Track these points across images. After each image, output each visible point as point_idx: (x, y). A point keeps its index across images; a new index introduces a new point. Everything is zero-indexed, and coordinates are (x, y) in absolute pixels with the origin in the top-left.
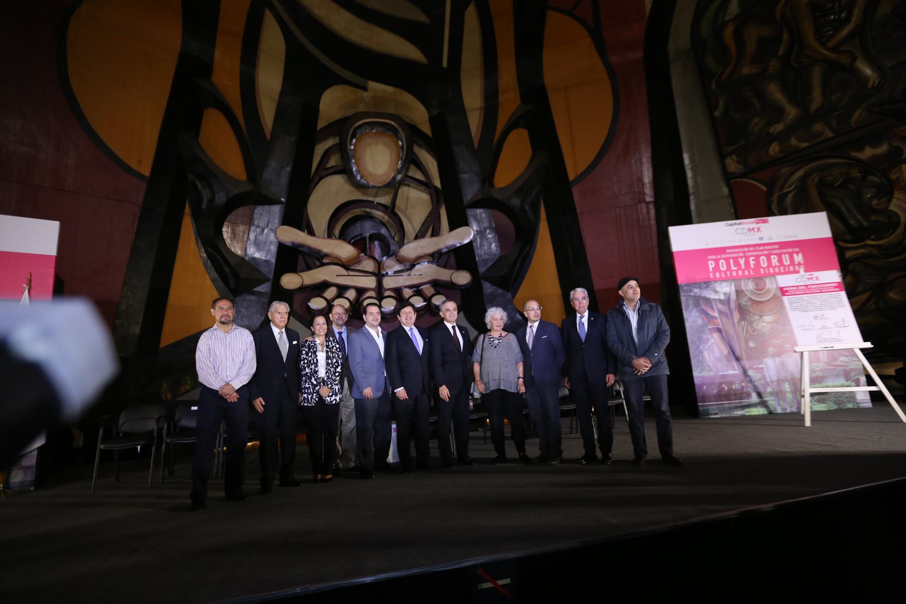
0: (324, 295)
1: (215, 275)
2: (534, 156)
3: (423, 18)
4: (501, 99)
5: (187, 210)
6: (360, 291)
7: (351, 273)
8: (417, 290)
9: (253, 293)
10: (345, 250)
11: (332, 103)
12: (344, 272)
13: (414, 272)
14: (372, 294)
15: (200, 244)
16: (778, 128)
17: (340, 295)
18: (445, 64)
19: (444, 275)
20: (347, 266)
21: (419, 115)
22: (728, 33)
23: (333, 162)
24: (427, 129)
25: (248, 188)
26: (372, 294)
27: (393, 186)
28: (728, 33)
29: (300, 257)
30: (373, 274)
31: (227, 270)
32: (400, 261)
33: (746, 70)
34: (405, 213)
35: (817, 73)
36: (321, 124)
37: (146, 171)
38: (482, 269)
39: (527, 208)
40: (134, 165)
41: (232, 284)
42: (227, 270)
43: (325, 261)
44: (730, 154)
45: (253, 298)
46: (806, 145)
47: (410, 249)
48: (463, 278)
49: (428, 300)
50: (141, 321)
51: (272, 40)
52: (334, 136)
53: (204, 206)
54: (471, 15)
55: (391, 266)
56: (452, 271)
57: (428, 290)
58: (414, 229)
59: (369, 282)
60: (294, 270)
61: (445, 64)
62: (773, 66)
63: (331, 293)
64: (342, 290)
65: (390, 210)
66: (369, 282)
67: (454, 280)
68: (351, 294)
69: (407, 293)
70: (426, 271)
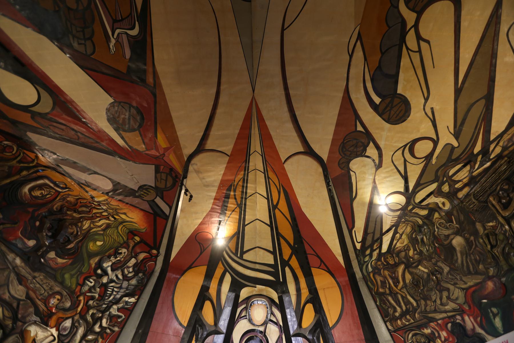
2: (315, 316)
3: (272, 270)
4: (302, 291)
5: (194, 338)
11: (244, 293)
16: (397, 314)
18: (281, 280)
21: (275, 296)
22: (371, 275)
23: (243, 315)
24: (277, 301)
25: (213, 329)
27: (265, 324)
28: (371, 275)
33: (381, 290)
34: (269, 335)
35: (399, 296)
36: (240, 300)
37: (185, 325)
39: (315, 338)
40: (183, 323)
44: (387, 321)
46: (407, 323)
51: (228, 279)
52: (244, 304)
54: (287, 269)
61: (281, 280)
62: (388, 291)
65: (264, 333)
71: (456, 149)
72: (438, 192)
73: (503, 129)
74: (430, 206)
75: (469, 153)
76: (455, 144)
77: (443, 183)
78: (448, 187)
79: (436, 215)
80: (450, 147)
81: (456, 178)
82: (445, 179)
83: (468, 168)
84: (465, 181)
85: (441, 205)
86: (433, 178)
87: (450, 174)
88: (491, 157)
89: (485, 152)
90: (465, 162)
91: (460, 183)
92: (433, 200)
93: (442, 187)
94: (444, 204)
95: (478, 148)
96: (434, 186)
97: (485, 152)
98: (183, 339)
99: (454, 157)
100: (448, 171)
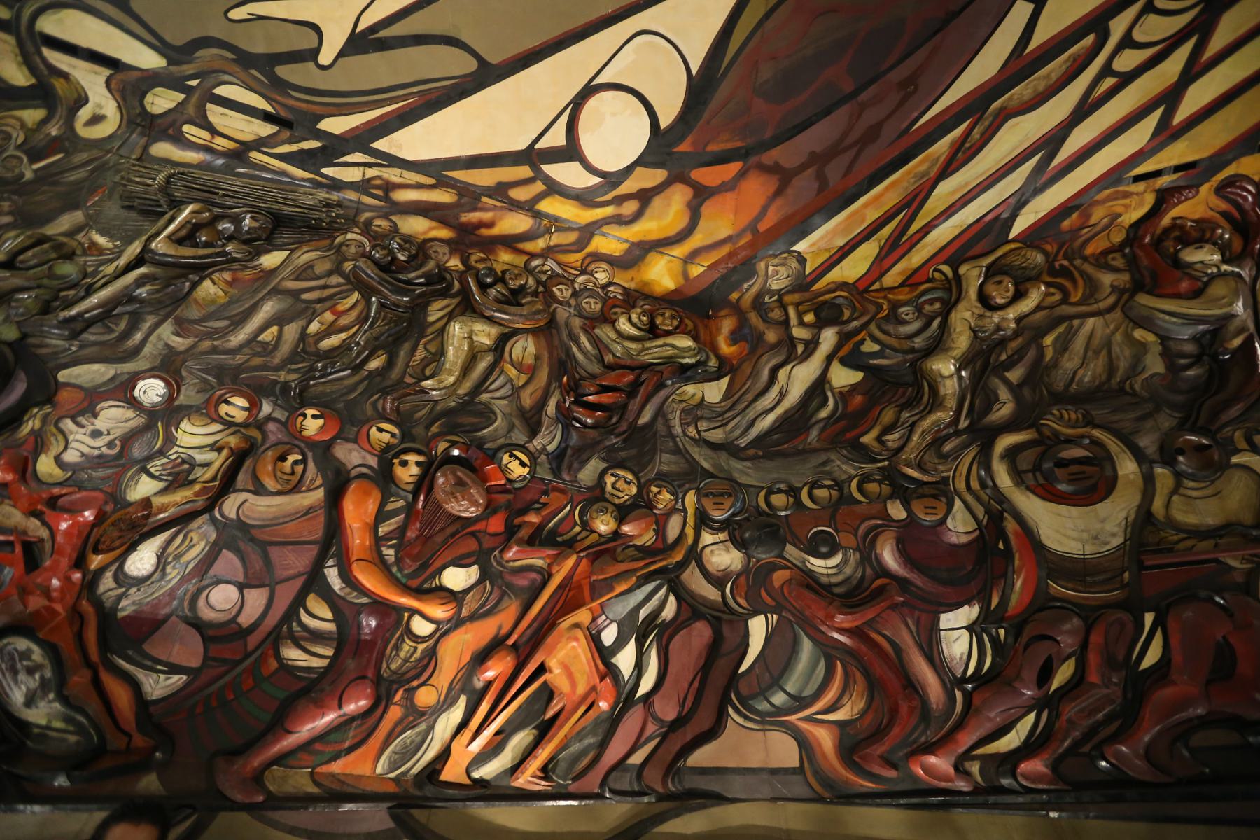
71: (311, 65)
72: (129, 85)
73: (411, 157)
74: (59, 84)
75: (314, 107)
76: (325, 57)
77: (176, 84)
78: (172, 105)
79: (32, 115)
80: (309, 41)
81: (216, 114)
82: (194, 83)
83: (267, 129)
84: (221, 143)
85: (84, 114)
86: (177, 37)
87: (221, 91)
88: (324, 171)
89: (334, 148)
90: (283, 113)
91: (205, 135)
92: (92, 80)
93: (158, 90)
94: (96, 119)
95: (335, 125)
96: (147, 59)
97: (334, 148)
99: (283, 71)
100: (226, 78)
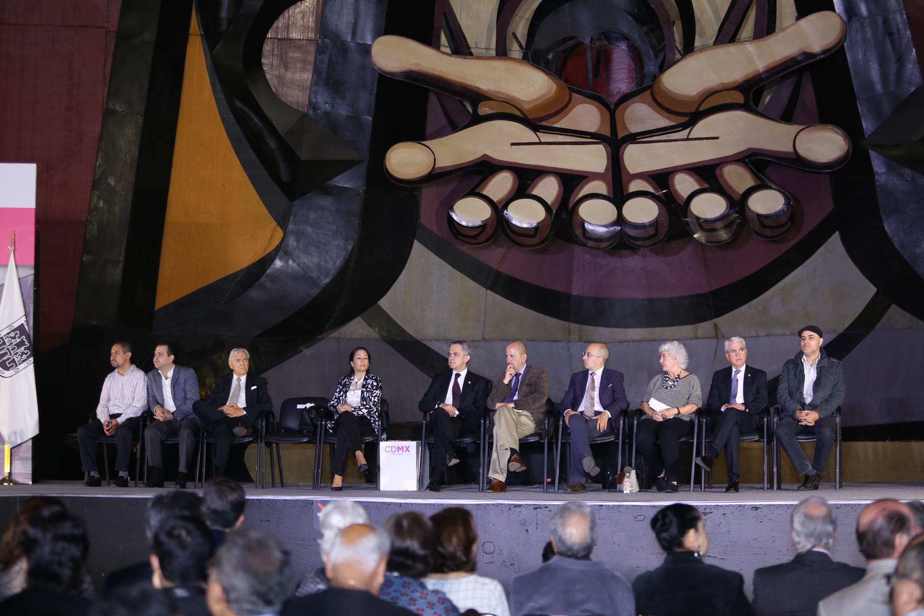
0: (485, 193)
1: (252, 155)
6: (571, 181)
7: (545, 138)
8: (708, 175)
9: (328, 191)
10: (530, 84)
12: (530, 136)
13: (700, 129)
14: (598, 186)
15: (219, 87)
17: (522, 191)
19: (773, 136)
20: (537, 120)
26: (598, 186)
29: (433, 100)
30: (596, 137)
31: (272, 143)
32: (664, 103)
38: (868, 125)
41: (284, 175)
42: (272, 143)
43: (484, 110)
45: (327, 202)
47: (687, 78)
48: (825, 145)
49: (738, 203)
50: (122, 258)
53: (224, 14)
55: (641, 115)
56: (794, 129)
57: (738, 178)
58: (716, 11)
59: (593, 158)
60: (418, 135)
63: (500, 185)
64: (526, 178)
66: (593, 158)
67: (802, 151)
68: (549, 189)
69: (684, 185)
70: (731, 133)
98: (124, 37)
